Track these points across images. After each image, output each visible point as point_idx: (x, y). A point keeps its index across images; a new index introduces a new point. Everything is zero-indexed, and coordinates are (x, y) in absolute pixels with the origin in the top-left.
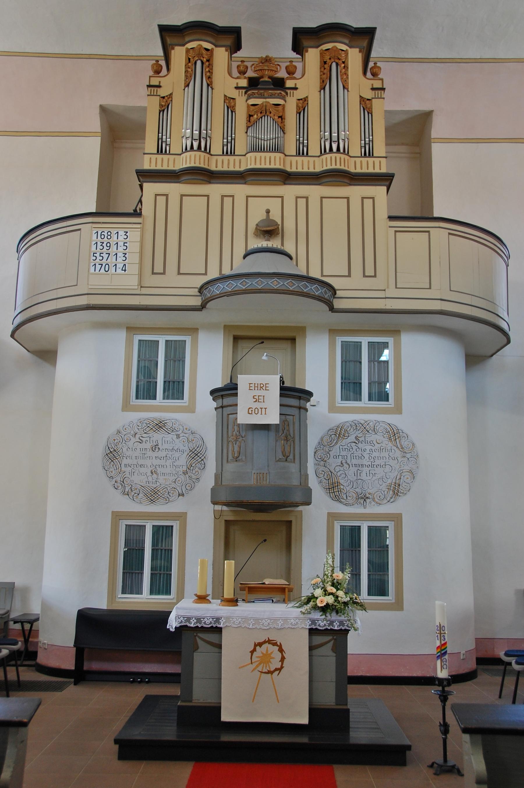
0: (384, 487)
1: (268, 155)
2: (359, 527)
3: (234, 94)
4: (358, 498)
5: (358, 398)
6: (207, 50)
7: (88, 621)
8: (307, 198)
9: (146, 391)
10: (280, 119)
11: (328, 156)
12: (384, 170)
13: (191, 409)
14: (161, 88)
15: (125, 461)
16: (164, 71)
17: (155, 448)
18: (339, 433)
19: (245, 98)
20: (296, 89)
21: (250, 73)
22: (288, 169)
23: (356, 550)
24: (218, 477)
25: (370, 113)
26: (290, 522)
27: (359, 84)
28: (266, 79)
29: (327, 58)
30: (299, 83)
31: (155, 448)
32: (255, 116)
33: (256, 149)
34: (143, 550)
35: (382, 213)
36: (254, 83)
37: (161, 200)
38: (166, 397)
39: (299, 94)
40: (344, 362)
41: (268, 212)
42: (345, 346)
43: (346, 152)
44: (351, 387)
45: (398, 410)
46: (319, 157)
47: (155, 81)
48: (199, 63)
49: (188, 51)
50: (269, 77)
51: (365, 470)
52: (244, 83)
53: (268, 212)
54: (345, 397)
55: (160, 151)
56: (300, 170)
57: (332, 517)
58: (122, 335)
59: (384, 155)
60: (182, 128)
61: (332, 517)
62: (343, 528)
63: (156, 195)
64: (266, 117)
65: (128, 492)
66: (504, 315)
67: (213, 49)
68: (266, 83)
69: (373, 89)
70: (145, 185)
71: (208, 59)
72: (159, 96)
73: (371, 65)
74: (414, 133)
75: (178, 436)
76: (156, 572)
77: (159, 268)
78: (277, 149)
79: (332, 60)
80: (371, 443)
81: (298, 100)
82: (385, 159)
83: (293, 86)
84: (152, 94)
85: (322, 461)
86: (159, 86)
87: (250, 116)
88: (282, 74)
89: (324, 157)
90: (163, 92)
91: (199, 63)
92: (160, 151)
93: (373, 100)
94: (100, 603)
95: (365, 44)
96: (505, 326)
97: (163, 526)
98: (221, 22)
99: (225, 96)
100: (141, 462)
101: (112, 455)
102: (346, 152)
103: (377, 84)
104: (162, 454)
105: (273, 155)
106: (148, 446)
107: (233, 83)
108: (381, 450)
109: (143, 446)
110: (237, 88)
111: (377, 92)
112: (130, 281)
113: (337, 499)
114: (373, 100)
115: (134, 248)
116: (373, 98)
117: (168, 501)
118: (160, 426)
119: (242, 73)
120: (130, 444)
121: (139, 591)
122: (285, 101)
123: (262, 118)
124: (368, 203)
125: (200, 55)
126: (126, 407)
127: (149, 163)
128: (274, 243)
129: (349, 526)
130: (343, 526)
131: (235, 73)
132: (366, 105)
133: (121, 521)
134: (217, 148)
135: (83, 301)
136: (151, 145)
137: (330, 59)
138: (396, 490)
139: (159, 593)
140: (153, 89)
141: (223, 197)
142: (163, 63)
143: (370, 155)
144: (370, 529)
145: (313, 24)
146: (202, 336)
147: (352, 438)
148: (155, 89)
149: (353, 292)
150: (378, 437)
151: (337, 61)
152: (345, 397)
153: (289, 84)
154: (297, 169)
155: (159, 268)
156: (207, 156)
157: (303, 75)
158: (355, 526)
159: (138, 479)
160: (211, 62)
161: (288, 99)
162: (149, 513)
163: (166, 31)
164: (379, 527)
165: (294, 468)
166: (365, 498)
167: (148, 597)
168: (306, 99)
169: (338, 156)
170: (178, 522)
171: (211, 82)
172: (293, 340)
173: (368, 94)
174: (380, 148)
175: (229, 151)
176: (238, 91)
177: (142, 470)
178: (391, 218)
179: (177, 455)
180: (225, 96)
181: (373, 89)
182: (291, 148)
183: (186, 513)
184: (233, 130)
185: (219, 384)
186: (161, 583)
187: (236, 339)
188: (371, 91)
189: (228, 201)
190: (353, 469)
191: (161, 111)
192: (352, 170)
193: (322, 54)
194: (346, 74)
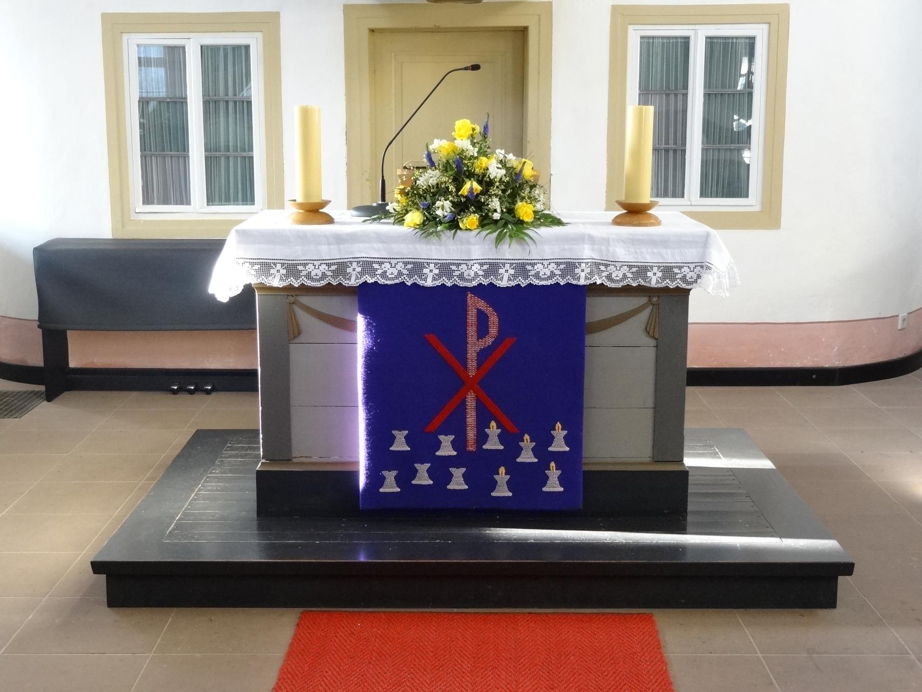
2: (686, 40)
23: (676, 95)
26: (523, 32)
62: (647, 43)
76: (218, 154)
97: (225, 48)
121: (183, 198)
129: (663, 38)
130: (649, 38)
133: (125, 37)
144: (711, 42)
158: (676, 38)
164: (732, 38)
167: (202, 211)
170: (259, 35)
183: (278, 14)
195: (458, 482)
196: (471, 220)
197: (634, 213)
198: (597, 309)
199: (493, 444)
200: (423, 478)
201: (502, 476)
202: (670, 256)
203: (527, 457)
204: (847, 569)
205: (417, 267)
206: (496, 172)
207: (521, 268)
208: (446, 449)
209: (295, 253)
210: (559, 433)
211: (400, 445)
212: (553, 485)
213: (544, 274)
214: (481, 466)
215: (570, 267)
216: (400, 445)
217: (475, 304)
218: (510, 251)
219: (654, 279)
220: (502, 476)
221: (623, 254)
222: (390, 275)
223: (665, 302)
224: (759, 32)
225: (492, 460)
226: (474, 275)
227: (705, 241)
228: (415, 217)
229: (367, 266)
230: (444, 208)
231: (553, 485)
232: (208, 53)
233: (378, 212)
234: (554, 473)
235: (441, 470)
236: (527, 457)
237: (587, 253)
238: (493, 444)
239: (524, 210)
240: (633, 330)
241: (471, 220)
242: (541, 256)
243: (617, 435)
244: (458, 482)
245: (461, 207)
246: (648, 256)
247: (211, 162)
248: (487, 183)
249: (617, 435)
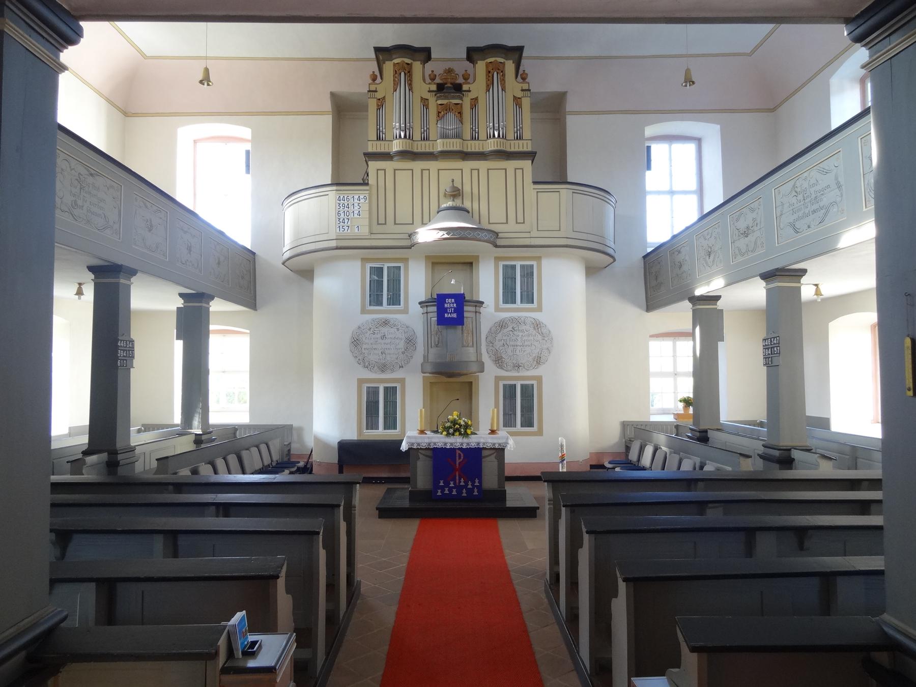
0: (531, 359)
4: (514, 367)
5: (514, 302)
7: (345, 448)
9: (376, 299)
11: (492, 140)
12: (530, 149)
13: (405, 311)
15: (364, 346)
16: (379, 80)
17: (383, 337)
18: (502, 325)
19: (435, 98)
20: (469, 91)
21: (438, 80)
22: (465, 150)
24: (426, 358)
25: (520, 107)
27: (514, 86)
28: (449, 85)
29: (490, 69)
30: (472, 87)
31: (383, 337)
33: (444, 136)
34: (377, 402)
35: (529, 178)
36: (441, 88)
37: (381, 173)
38: (389, 304)
39: (472, 95)
40: (505, 278)
41: (453, 181)
42: (505, 267)
43: (504, 137)
44: (509, 296)
45: (539, 309)
47: (373, 88)
48: (403, 74)
49: (395, 65)
51: (519, 348)
52: (434, 87)
53: (453, 181)
54: (506, 301)
55: (379, 138)
56: (473, 150)
57: (498, 379)
58: (358, 264)
60: (395, 125)
61: (498, 379)
62: (505, 386)
65: (367, 366)
66: (611, 244)
68: (449, 87)
69: (522, 90)
70: (370, 163)
73: (521, 72)
74: (553, 108)
75: (398, 329)
77: (382, 221)
78: (458, 136)
80: (522, 331)
85: (491, 343)
86: (376, 91)
87: (439, 112)
88: (460, 80)
89: (489, 141)
90: (379, 95)
91: (403, 74)
92: (379, 138)
94: (352, 435)
95: (517, 56)
96: (610, 251)
98: (417, 44)
100: (375, 346)
101: (356, 342)
102: (504, 137)
103: (525, 86)
104: (388, 341)
105: (455, 140)
106: (379, 336)
107: (427, 87)
108: (528, 335)
109: (376, 336)
112: (365, 231)
113: (501, 367)
115: (366, 207)
117: (393, 371)
118: (386, 323)
119: (433, 78)
120: (367, 335)
124: (519, 172)
126: (364, 311)
127: (373, 147)
128: (458, 202)
131: (428, 80)
132: (517, 101)
134: (417, 136)
135: (333, 244)
136: (372, 135)
138: (538, 361)
139: (389, 429)
142: (377, 73)
143: (520, 138)
144: (522, 386)
145: (482, 44)
146: (412, 264)
147: (510, 328)
149: (509, 230)
150: (527, 327)
152: (506, 301)
153: (465, 87)
155: (382, 221)
157: (474, 81)
159: (373, 358)
161: (464, 98)
162: (381, 379)
163: (378, 50)
165: (472, 350)
166: (519, 366)
168: (476, 99)
169: (499, 140)
172: (471, 264)
173: (519, 94)
174: (527, 134)
175: (426, 139)
177: (376, 352)
178: (535, 183)
179: (397, 341)
181: (522, 90)
182: (467, 135)
184: (428, 123)
185: (424, 300)
186: (391, 423)
187: (434, 264)
189: (426, 173)
190: (511, 348)
191: (378, 109)
192: (508, 149)
193: (487, 65)
194: (504, 80)
195: (454, 493)
196: (457, 433)
197: (493, 432)
198: (484, 453)
199: (462, 484)
200: (447, 492)
201: (464, 491)
202: (500, 442)
203: (470, 486)
204: (538, 508)
205: (446, 444)
206: (463, 423)
207: (468, 444)
208: (452, 485)
209: (419, 441)
210: (477, 481)
211: (442, 484)
212: (476, 493)
213: (473, 445)
214: (459, 488)
215: (478, 444)
216: (442, 484)
217: (458, 452)
218: (465, 440)
219: (497, 446)
220: (464, 491)
221: (490, 441)
222: (440, 445)
223: (499, 452)
224: (534, 382)
225: (463, 487)
226: (458, 446)
227: (507, 439)
228: (445, 433)
229: (435, 444)
230: (451, 431)
231: (476, 493)
232: (386, 389)
233: (436, 432)
234: (476, 490)
235: (451, 490)
236: (470, 486)
237: (482, 441)
238: (462, 484)
239: (469, 431)
240: (493, 458)
241: (457, 433)
242: (473, 441)
243: (490, 480)
244: (454, 493)
245: (455, 431)
246: (495, 441)
247: (385, 418)
248: (461, 426)
249: (490, 480)
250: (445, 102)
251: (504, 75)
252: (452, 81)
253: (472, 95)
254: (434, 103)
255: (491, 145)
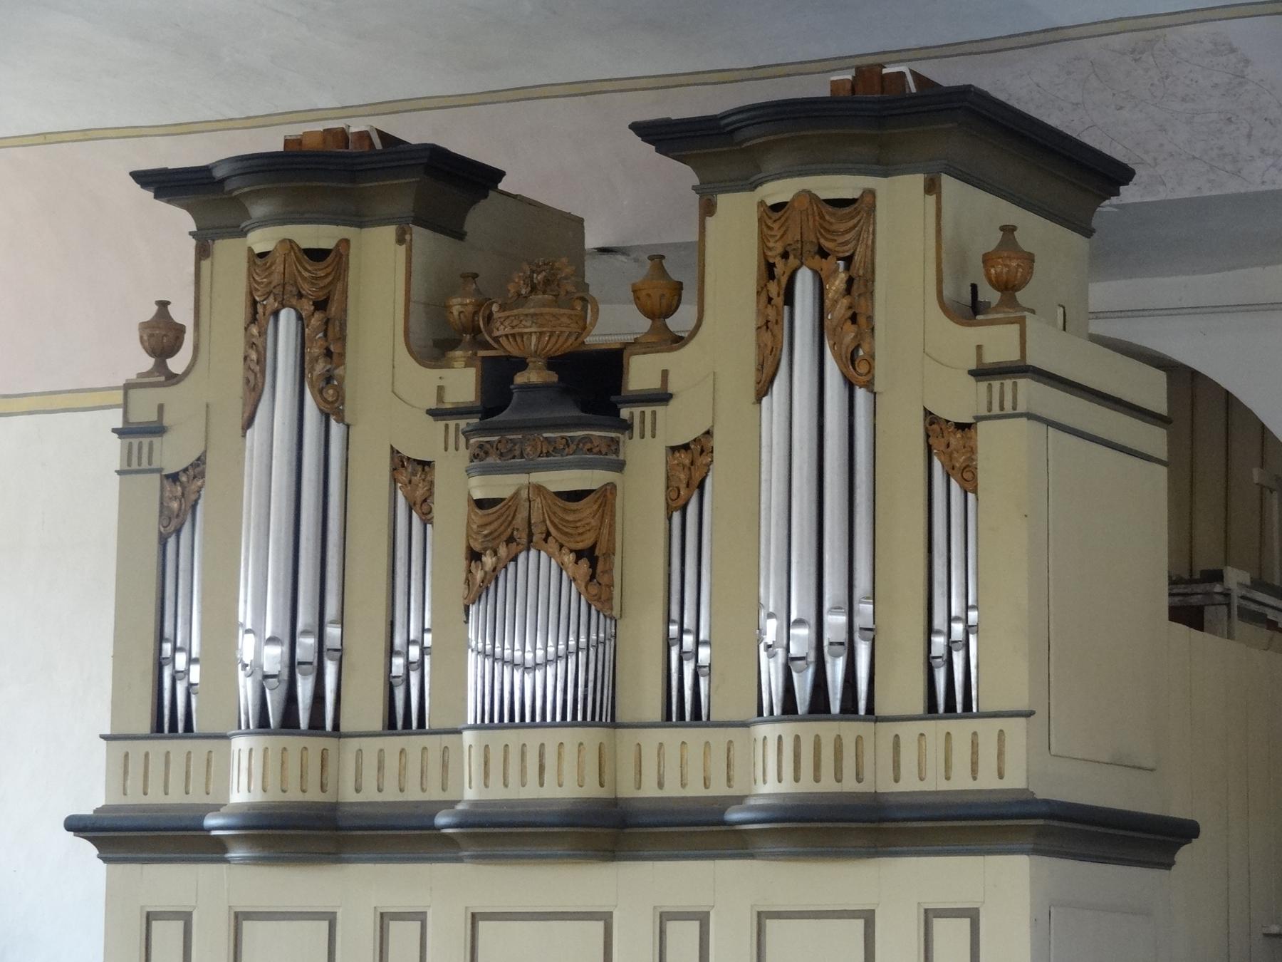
1: (533, 738)
3: (426, 440)
6: (317, 255)
8: (703, 919)
10: (584, 565)
14: (167, 437)
20: (662, 397)
30: (681, 366)
32: (488, 560)
39: (677, 424)
46: (745, 725)
50: (553, 363)
52: (462, 383)
56: (673, 790)
59: (1023, 705)
63: (150, 917)
64: (533, 553)
67: (345, 242)
71: (321, 295)
72: (159, 470)
79: (793, 261)
81: (674, 449)
82: (1022, 720)
83: (653, 383)
84: (135, 466)
86: (157, 430)
87: (474, 556)
88: (615, 322)
93: (981, 425)
99: (394, 451)
107: (423, 384)
110: (436, 414)
111: (996, 384)
114: (981, 425)
116: (979, 419)
122: (619, 466)
123: (515, 559)
125: (286, 294)
137: (785, 255)
140: (135, 442)
141: (384, 919)
148: (146, 441)
151: (817, 261)
153: (641, 373)
154: (661, 785)
156: (316, 744)
160: (333, 309)
171: (340, 396)
173: (960, 400)
176: (441, 424)
180: (394, 451)
181: (982, 373)
188: (972, 379)
250: (502, 486)
251: (860, 284)
252: (564, 345)
253: (677, 424)
254: (459, 484)
255: (773, 768)
